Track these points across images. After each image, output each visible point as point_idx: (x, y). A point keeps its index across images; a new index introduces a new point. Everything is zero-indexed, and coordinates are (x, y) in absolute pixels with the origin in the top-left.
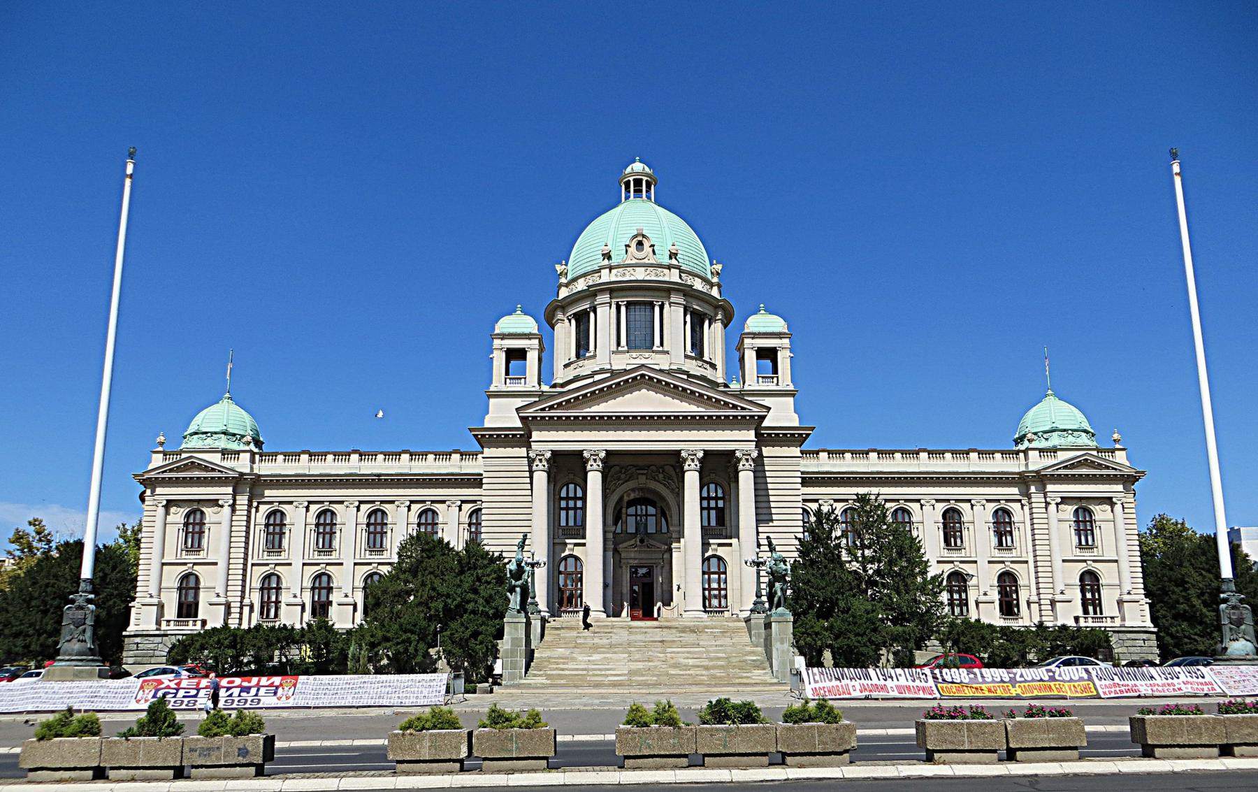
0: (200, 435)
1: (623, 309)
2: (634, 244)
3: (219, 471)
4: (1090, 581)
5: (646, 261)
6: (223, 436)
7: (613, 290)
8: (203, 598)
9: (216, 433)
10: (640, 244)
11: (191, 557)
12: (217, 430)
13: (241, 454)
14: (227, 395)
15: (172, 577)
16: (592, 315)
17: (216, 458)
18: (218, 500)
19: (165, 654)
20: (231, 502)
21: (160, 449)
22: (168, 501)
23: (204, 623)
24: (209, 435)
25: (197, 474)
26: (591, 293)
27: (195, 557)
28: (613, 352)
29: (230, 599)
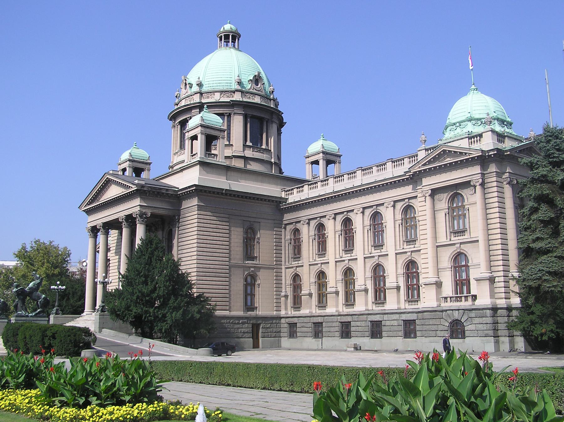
6: (469, 124)
8: (474, 274)
11: (460, 238)
12: (464, 118)
13: (483, 134)
14: (473, 87)
15: (446, 256)
17: (465, 144)
19: (446, 328)
20: (481, 181)
21: (423, 147)
22: (432, 190)
23: (474, 297)
24: (458, 124)
25: (449, 160)
27: (462, 237)
29: (495, 274)
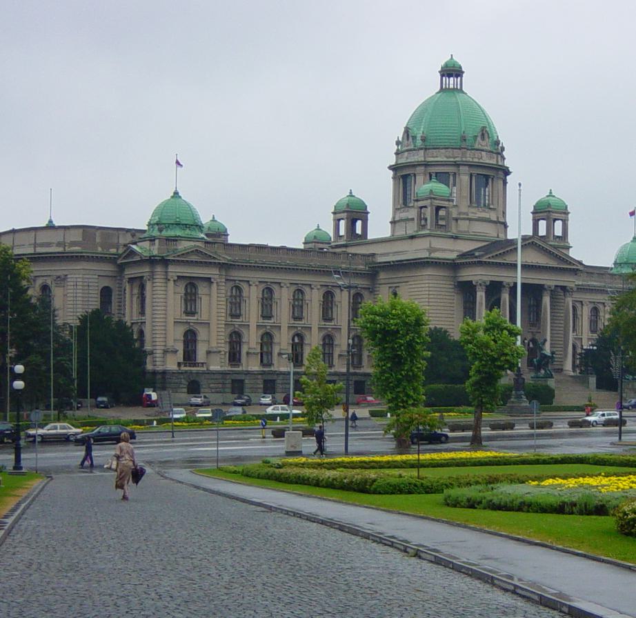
0: (181, 226)
1: (474, 178)
2: (480, 134)
3: (214, 258)
4: (190, 339)
5: (486, 148)
7: (470, 166)
9: (192, 225)
10: (483, 135)
12: (192, 223)
15: (181, 330)
16: (451, 178)
18: (210, 278)
22: (178, 277)
26: (457, 165)
28: (469, 206)
